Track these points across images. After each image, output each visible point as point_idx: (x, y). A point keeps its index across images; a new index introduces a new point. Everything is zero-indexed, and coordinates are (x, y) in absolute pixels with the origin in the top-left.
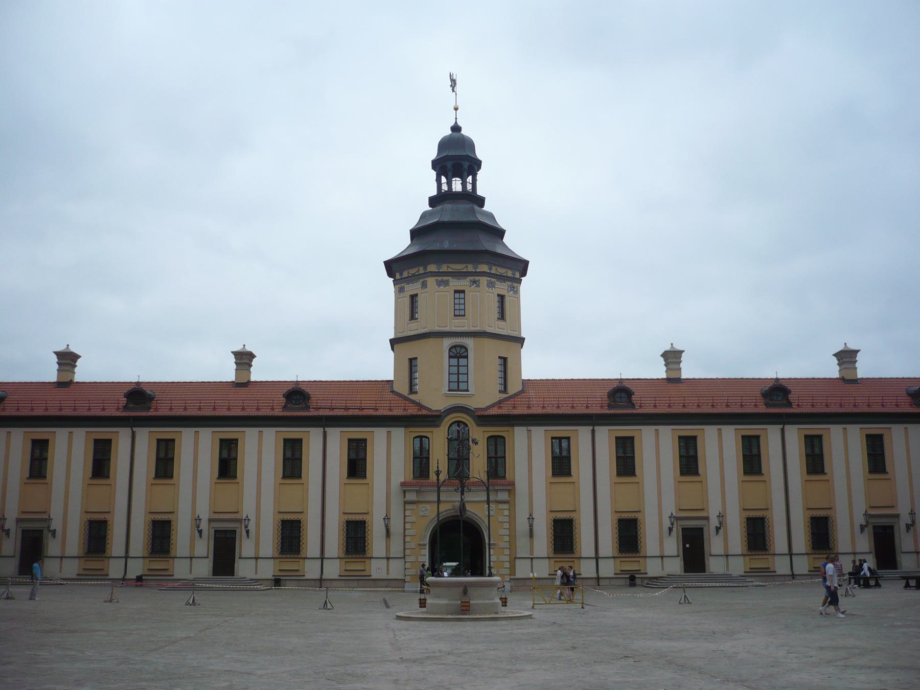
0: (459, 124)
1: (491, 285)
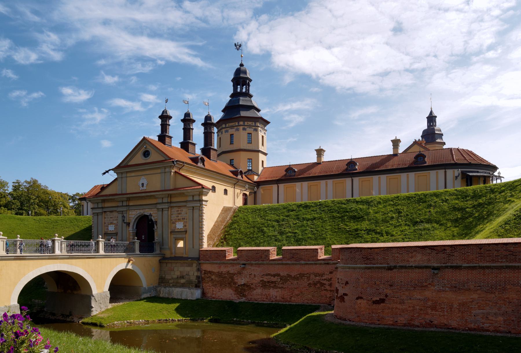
1: (244, 129)
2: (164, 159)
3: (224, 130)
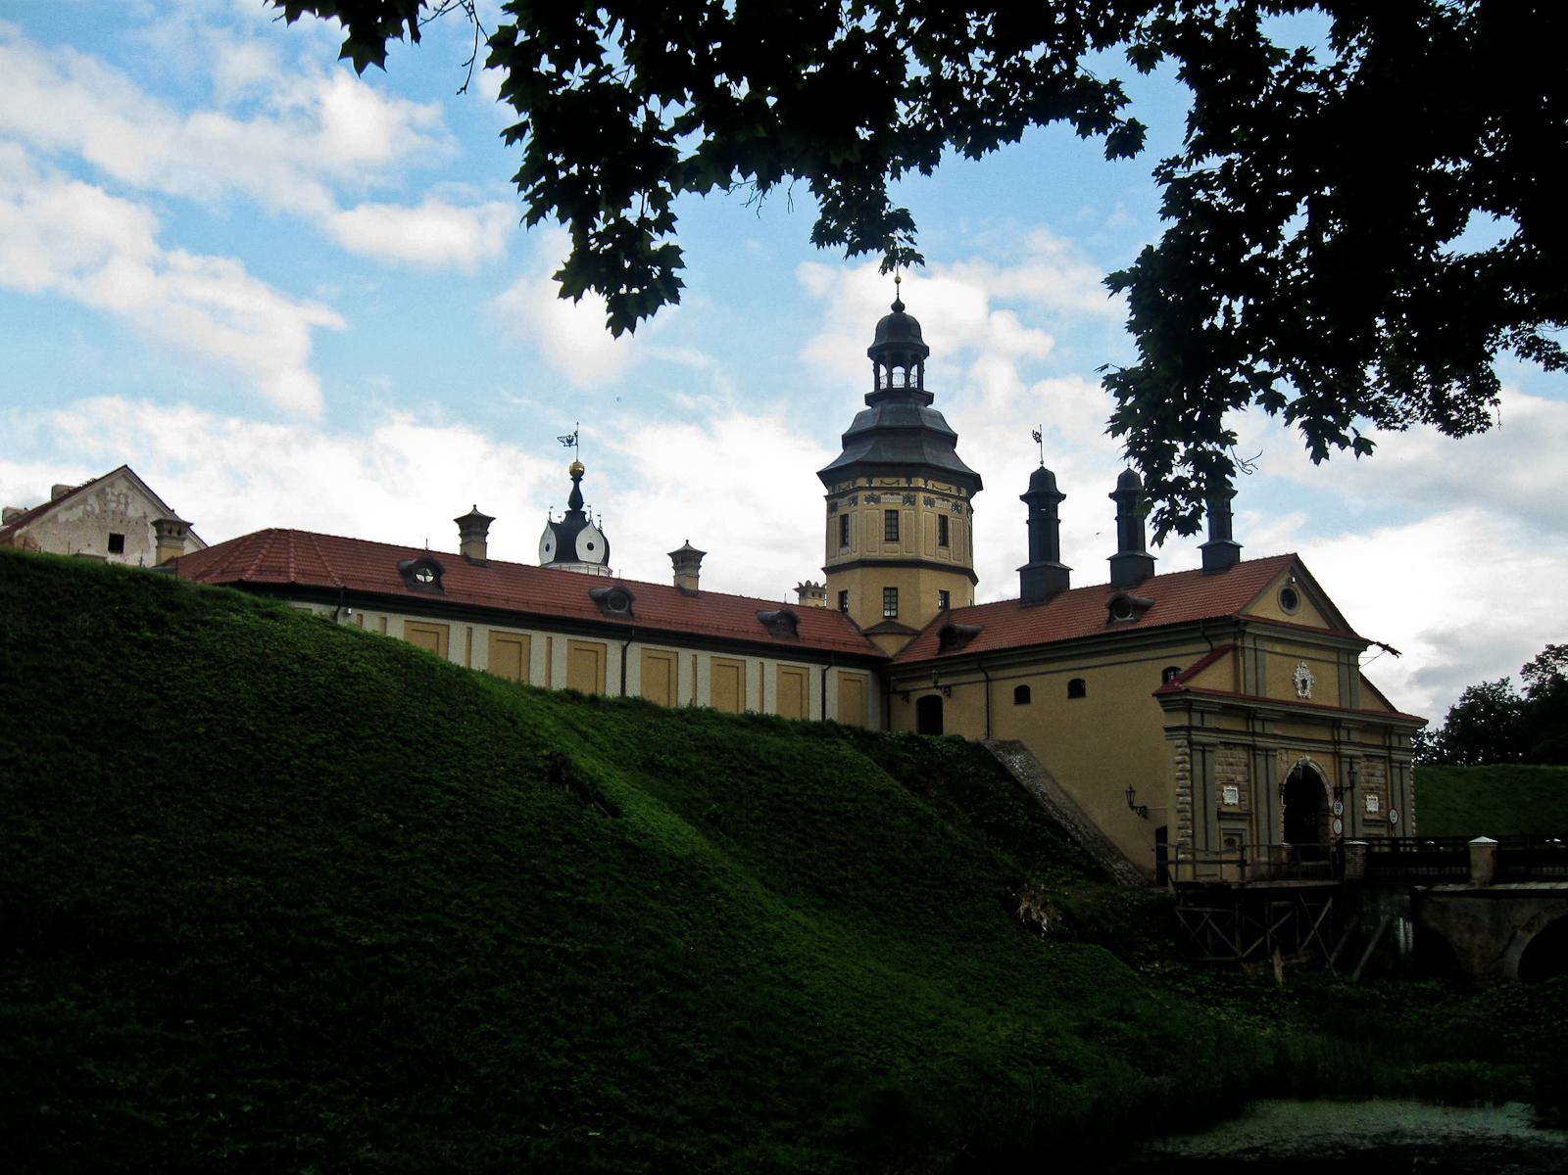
0: (902, 300)
2: (1326, 627)
3: (921, 496)
